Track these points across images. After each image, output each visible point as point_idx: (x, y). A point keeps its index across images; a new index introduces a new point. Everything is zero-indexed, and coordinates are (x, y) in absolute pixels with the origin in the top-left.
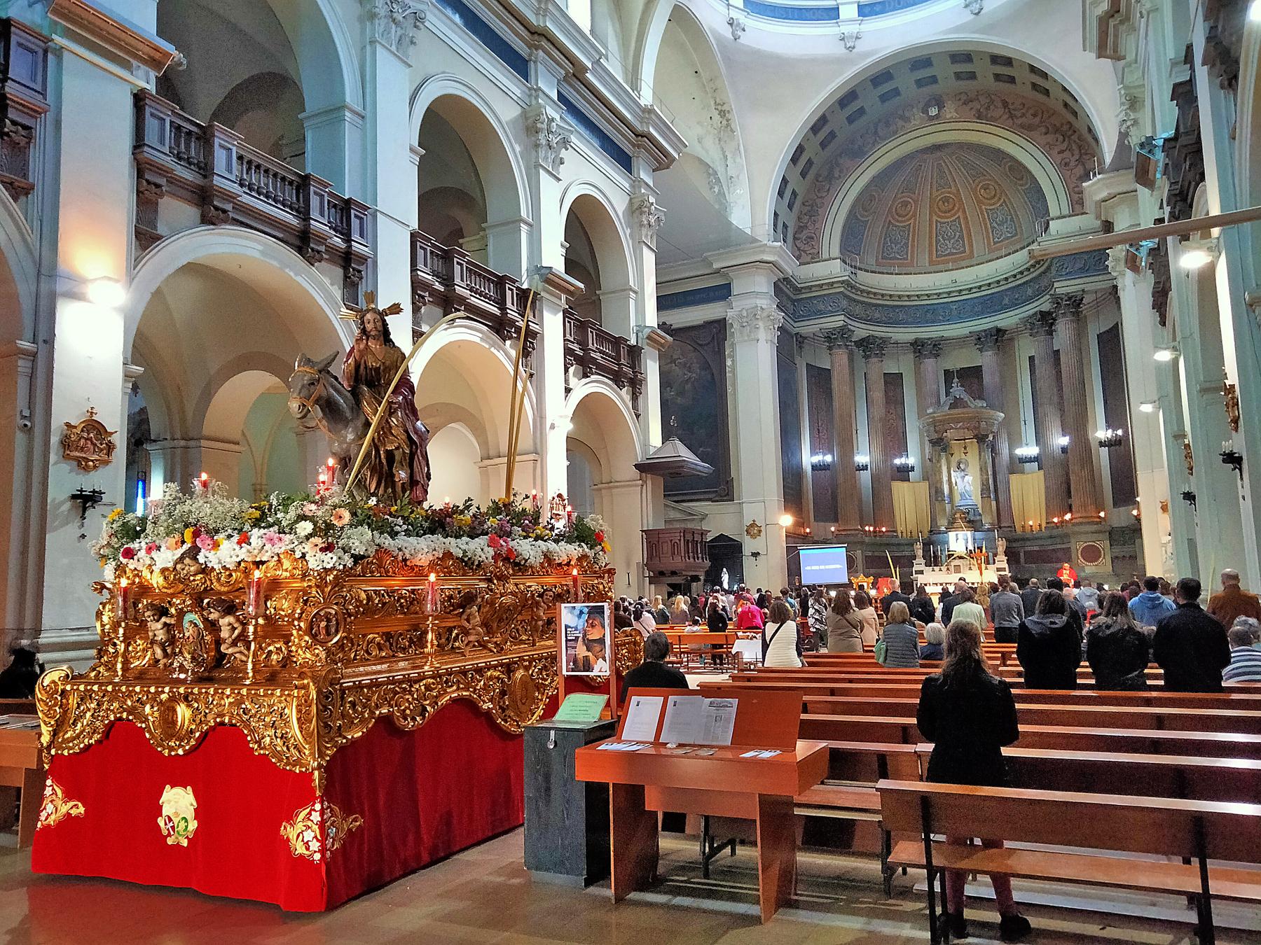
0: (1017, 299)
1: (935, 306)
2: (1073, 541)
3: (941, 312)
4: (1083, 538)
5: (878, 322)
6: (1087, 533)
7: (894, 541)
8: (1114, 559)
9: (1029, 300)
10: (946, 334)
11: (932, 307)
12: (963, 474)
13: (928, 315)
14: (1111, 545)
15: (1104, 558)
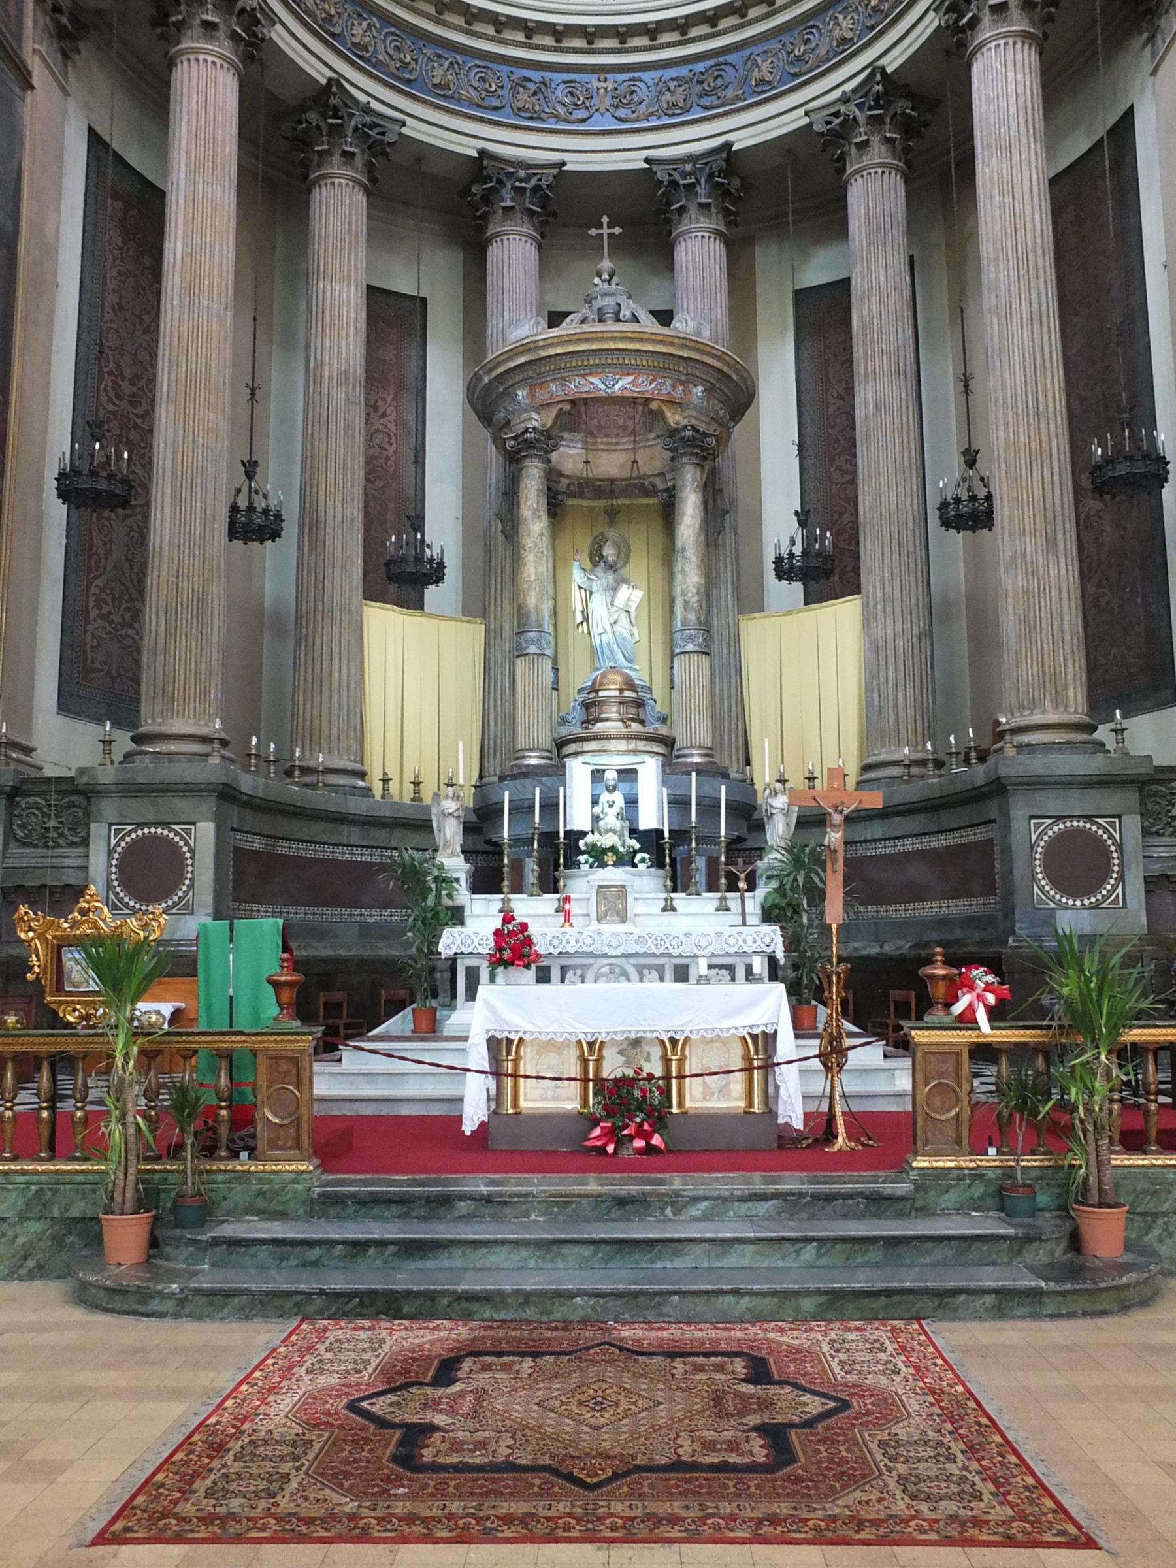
0: (799, 59)
1: (548, 75)
2: (1019, 811)
3: (561, 93)
4: (1053, 802)
5: (361, 57)
6: (1068, 783)
7: (356, 806)
8: (1153, 884)
9: (845, 49)
10: (574, 164)
11: (536, 75)
12: (610, 578)
13: (523, 97)
14: (1146, 833)
15: (1121, 879)
